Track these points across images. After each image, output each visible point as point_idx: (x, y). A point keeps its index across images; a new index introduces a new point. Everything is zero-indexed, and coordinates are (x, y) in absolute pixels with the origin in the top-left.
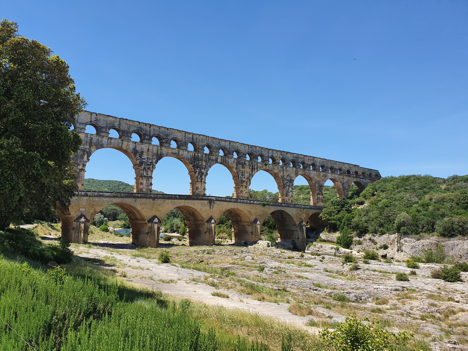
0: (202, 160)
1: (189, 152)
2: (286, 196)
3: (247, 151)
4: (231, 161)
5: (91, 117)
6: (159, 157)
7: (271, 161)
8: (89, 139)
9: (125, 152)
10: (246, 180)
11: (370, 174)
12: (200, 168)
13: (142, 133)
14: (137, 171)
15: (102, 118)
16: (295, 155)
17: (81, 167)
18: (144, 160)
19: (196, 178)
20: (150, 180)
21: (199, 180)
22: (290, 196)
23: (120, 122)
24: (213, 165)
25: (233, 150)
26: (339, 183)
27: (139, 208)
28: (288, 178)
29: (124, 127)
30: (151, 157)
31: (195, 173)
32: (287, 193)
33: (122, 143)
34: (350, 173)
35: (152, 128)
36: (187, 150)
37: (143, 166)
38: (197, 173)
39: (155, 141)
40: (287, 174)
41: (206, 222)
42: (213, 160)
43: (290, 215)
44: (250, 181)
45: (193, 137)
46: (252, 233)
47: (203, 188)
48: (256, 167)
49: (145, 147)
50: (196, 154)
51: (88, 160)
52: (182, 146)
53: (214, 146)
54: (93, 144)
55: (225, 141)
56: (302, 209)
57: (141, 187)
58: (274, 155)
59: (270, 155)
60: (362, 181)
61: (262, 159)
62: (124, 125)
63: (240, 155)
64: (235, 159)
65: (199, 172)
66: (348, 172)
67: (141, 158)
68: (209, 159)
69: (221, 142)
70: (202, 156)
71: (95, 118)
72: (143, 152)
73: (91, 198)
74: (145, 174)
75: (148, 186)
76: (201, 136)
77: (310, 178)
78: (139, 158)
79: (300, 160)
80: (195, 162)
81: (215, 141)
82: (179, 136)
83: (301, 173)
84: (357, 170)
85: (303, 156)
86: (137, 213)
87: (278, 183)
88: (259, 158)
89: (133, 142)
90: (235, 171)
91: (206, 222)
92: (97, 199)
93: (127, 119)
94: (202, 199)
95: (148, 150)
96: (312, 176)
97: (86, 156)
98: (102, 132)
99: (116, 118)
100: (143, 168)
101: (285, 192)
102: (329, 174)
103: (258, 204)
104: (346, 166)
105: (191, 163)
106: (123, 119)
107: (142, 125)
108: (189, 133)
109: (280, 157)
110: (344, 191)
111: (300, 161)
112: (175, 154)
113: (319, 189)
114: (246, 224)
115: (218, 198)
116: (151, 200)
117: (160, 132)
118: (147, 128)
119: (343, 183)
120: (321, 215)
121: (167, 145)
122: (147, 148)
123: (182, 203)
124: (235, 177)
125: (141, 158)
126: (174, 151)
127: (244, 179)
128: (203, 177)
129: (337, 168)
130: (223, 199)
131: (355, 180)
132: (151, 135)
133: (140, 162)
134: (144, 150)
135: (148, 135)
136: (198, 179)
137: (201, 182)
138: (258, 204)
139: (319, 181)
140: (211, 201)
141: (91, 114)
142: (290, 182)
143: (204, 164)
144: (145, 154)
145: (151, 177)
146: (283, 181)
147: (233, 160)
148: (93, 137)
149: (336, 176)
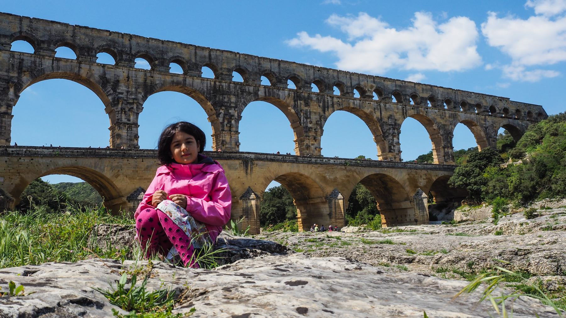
0: (229, 93)
1: (203, 79)
2: (390, 152)
3: (312, 77)
4: (282, 94)
5: (21, 24)
6: (150, 89)
7: (357, 95)
8: (17, 61)
9: (87, 82)
10: (315, 127)
11: (529, 113)
12: (225, 106)
13: (116, 50)
15: (41, 26)
16: (398, 83)
18: (121, 96)
19: (220, 125)
20: (134, 129)
21: (226, 128)
22: (396, 152)
24: (249, 101)
25: (286, 75)
26: (479, 128)
27: (108, 174)
28: (390, 121)
29: (82, 40)
31: (218, 115)
32: (390, 147)
33: (80, 68)
34: (495, 111)
35: (134, 41)
36: (200, 76)
37: (120, 106)
38: (221, 115)
40: (389, 113)
42: (249, 93)
43: (397, 183)
44: (321, 127)
45: (210, 55)
46: (330, 215)
47: (233, 142)
48: (330, 103)
49: (122, 73)
50: (217, 83)
51: (18, 97)
52: (191, 70)
53: (250, 70)
54: (24, 69)
55: (271, 60)
56: (419, 171)
57: (118, 141)
58: (362, 83)
59: (354, 83)
60: (518, 123)
61: (342, 90)
62: (83, 37)
63: (300, 85)
64: (290, 90)
65: (225, 115)
66: (492, 109)
67: (115, 91)
68: (243, 91)
69: (262, 62)
70: (229, 86)
71: (29, 26)
72: (118, 81)
73: (15, 159)
74: (124, 120)
75: (131, 140)
76: (225, 54)
77: (429, 120)
78: (112, 92)
79: (409, 91)
80: (215, 96)
81: (251, 61)
82: (185, 54)
83: (412, 112)
84: (506, 106)
85: (413, 85)
86: (109, 187)
87: (374, 132)
88: (335, 88)
89: (99, 65)
90: (293, 111)
91: (241, 198)
92: (27, 160)
93: (86, 28)
95: (128, 77)
96: (431, 116)
97: (12, 91)
98: (41, 48)
99: (67, 25)
100: (119, 109)
101: (387, 146)
102: (460, 114)
103: (337, 164)
104: (488, 99)
105: (209, 99)
106: (80, 27)
107: (115, 37)
108: (203, 49)
109: (372, 87)
110: (488, 139)
111: (409, 94)
112: (178, 83)
113: (447, 138)
114: (318, 200)
115: (260, 156)
116: (132, 161)
117: (149, 48)
119: (486, 128)
120: (452, 179)
121: (162, 69)
122: (125, 74)
124: (296, 124)
125: (115, 91)
126: (175, 79)
127: (310, 125)
128: (233, 122)
129: (473, 103)
130: (269, 157)
131: (505, 122)
132: (133, 52)
133: (114, 99)
134: (121, 78)
135: (128, 54)
136: (223, 126)
137: (230, 131)
138: (337, 164)
139: (444, 125)
140: (249, 161)
141: (21, 19)
142: (394, 129)
143: (233, 99)
145: (137, 125)
146: (382, 126)
147: (287, 92)
148: (25, 58)
149: (473, 116)
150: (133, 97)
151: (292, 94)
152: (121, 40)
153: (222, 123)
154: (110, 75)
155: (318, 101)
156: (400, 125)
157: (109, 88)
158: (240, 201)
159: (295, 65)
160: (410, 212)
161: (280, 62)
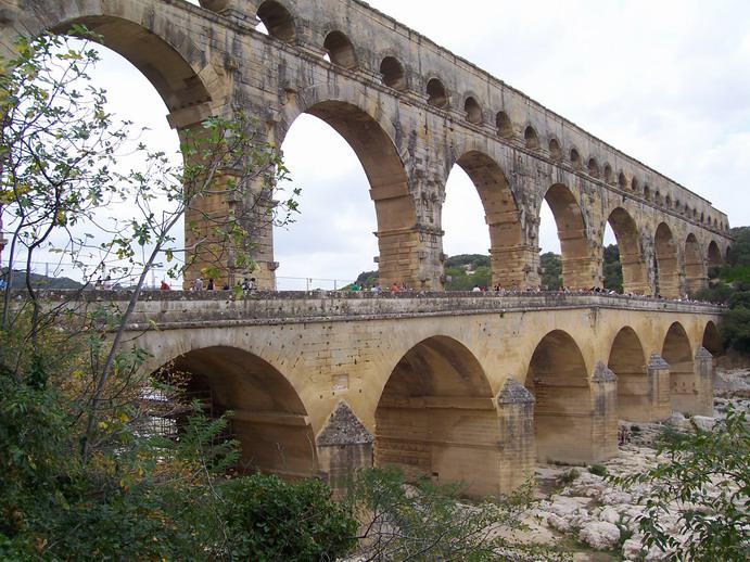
14: (390, 207)
17: (258, 185)
23: (348, 13)
27: (475, 348)
30: (433, 154)
33: (365, 94)
38: (523, 216)
41: (595, 377)
67: (412, 155)
72: (414, 133)
73: (362, 327)
74: (426, 222)
100: (419, 196)
125: (412, 155)
133: (411, 171)
144: (419, 140)
150: (434, 170)
153: (524, 230)
158: (591, 384)
159: (574, 129)
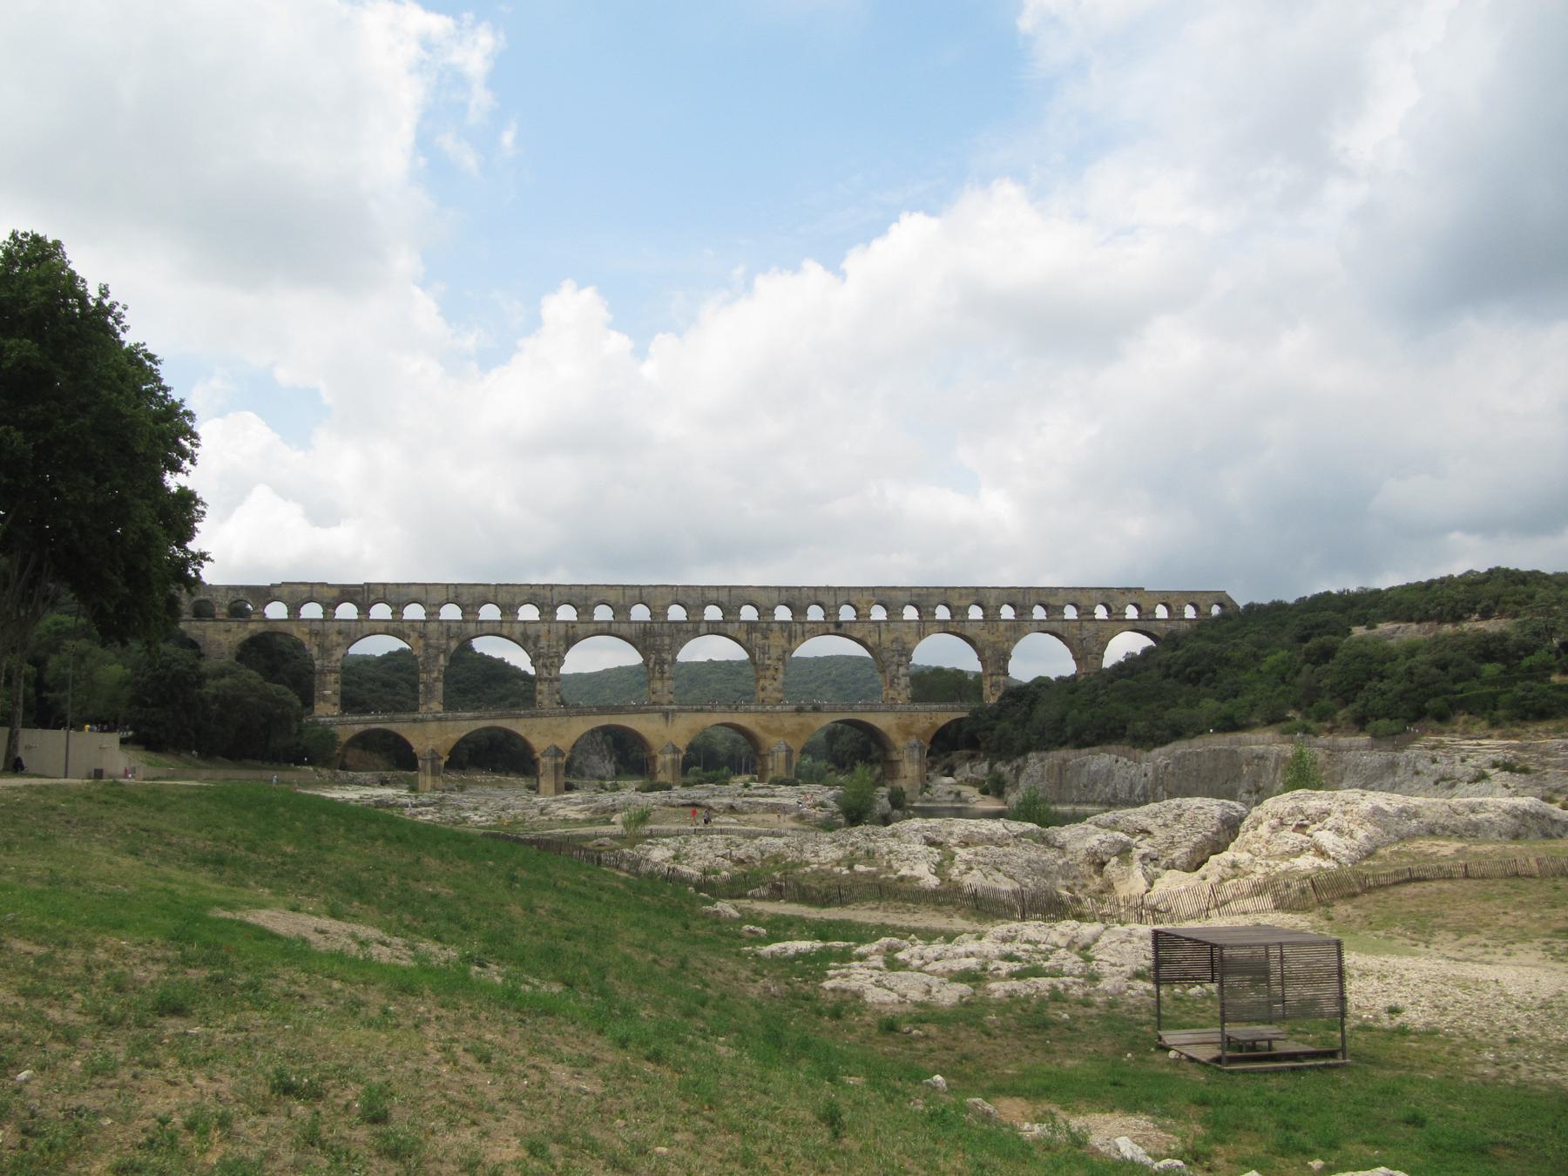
0: (661, 635)
4: (730, 628)
15: (465, 590)
17: (435, 675)
29: (504, 597)
32: (892, 682)
35: (555, 591)
39: (566, 613)
48: (799, 632)
55: (718, 588)
58: (853, 600)
74: (545, 675)
82: (612, 596)
94: (647, 711)
118: (548, 594)
121: (586, 618)
123: (605, 720)
143: (667, 641)
151: (744, 627)
152: (542, 592)
154: (531, 630)
155: (782, 630)
156: (911, 651)
157: (530, 644)
160: (901, 766)
161: (730, 588)
